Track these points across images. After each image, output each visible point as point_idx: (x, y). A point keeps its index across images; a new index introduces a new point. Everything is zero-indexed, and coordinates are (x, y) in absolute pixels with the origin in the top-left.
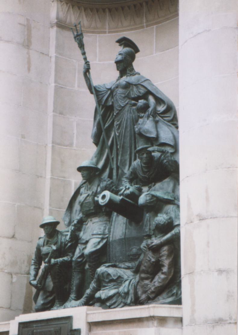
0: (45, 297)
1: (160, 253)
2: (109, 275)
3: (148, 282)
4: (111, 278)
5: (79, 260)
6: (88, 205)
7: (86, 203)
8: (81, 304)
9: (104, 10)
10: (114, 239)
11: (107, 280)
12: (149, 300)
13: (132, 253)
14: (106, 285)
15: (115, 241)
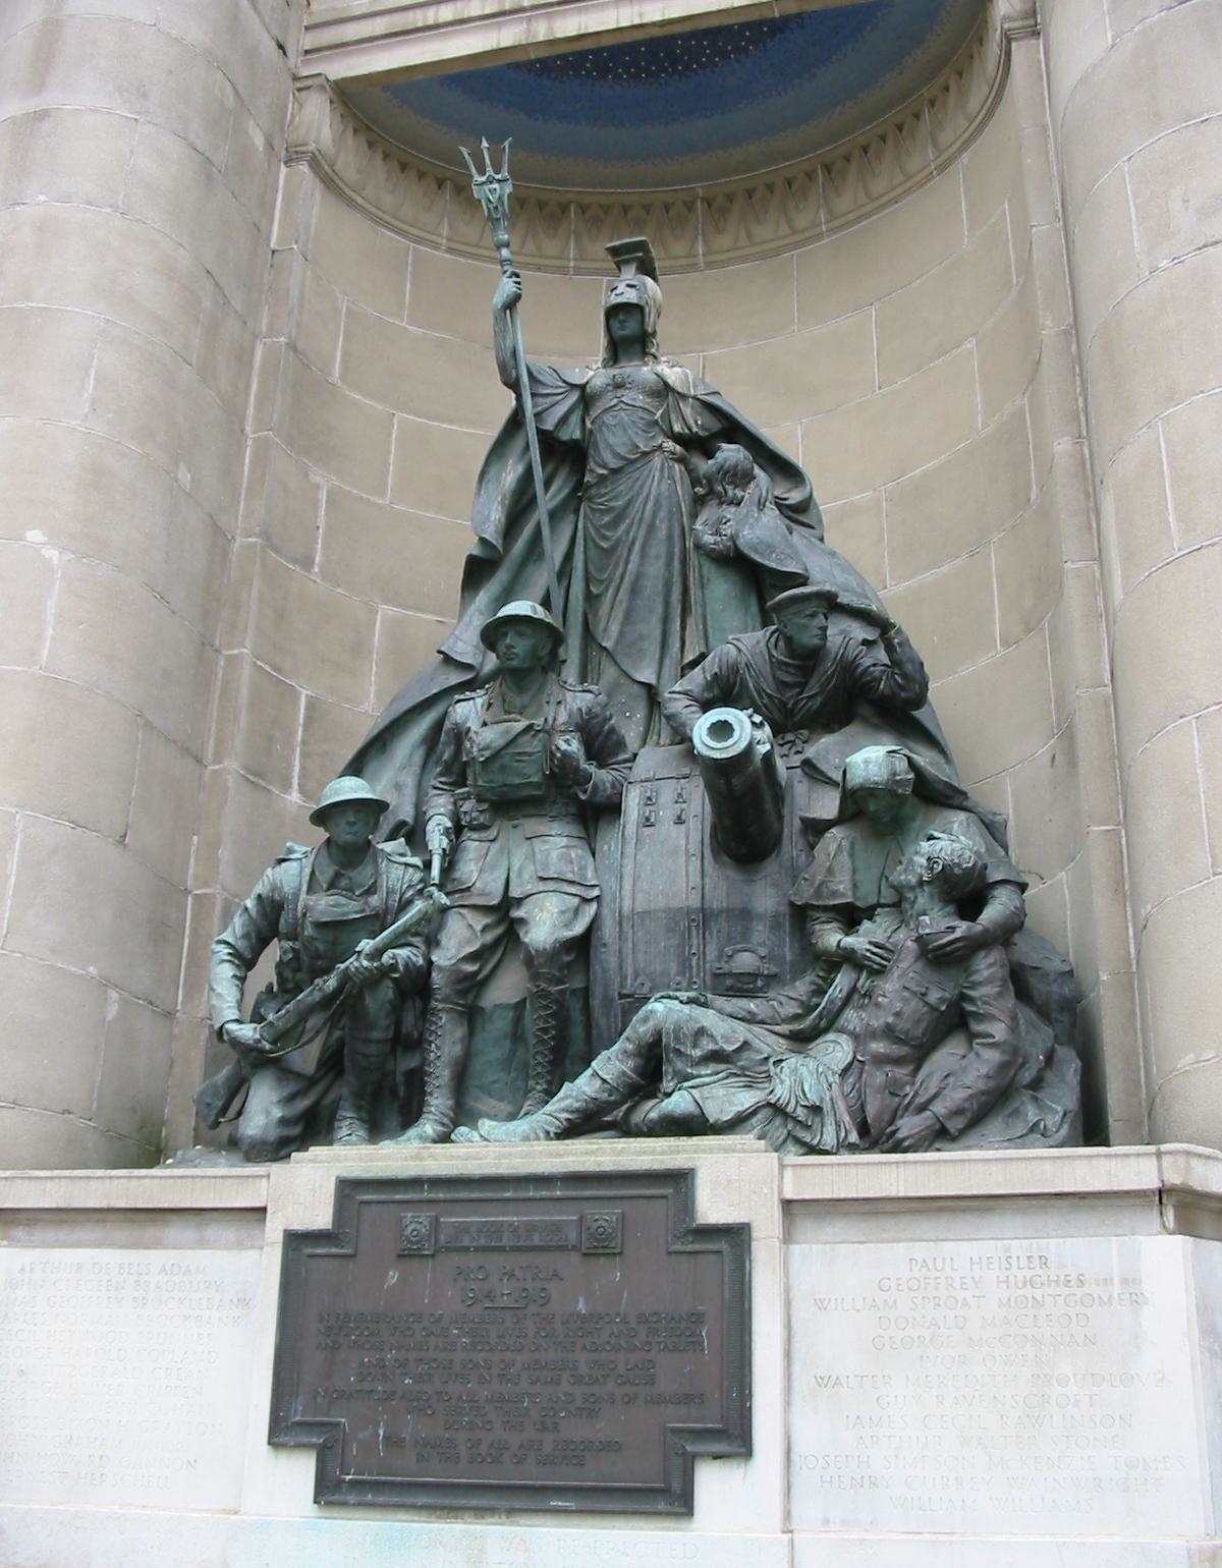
0: (285, 1093)
1: (968, 972)
2: (701, 1032)
3: (907, 1075)
4: (711, 1047)
5: (471, 968)
8: (542, 1135)
9: (440, 183)
11: (697, 1053)
12: (940, 1135)
15: (646, 913)
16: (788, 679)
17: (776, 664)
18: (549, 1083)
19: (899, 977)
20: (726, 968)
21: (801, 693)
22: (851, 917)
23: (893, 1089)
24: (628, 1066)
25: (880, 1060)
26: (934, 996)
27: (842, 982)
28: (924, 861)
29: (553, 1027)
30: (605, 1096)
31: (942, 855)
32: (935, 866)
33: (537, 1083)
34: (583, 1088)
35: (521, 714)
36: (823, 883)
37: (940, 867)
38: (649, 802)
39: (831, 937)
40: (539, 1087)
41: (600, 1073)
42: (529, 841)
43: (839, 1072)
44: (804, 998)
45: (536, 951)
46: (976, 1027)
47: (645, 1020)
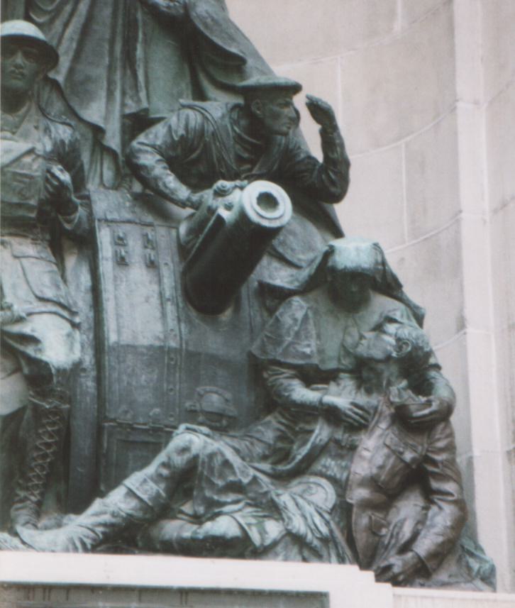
4: (231, 478)
6: (22, 185)
7: (15, 174)
8: (79, 545)
10: (126, 338)
11: (220, 483)
13: (206, 406)
14: (216, 497)
15: (132, 348)
16: (246, 155)
17: (239, 139)
18: (42, 494)
19: (381, 436)
20: (198, 408)
21: (250, 170)
22: (313, 376)
23: (374, 529)
24: (160, 488)
25: (366, 505)
26: (408, 456)
27: (321, 432)
28: (392, 340)
29: (56, 443)
30: (139, 514)
31: (411, 338)
32: (404, 346)
33: (33, 494)
34: (116, 503)
35: (14, 133)
36: (291, 344)
37: (409, 349)
38: (120, 242)
39: (301, 393)
40: (33, 498)
41: (139, 493)
42: (17, 261)
43: (329, 511)
44: (271, 442)
45: (58, 370)
46: (435, 485)
47: (185, 450)
